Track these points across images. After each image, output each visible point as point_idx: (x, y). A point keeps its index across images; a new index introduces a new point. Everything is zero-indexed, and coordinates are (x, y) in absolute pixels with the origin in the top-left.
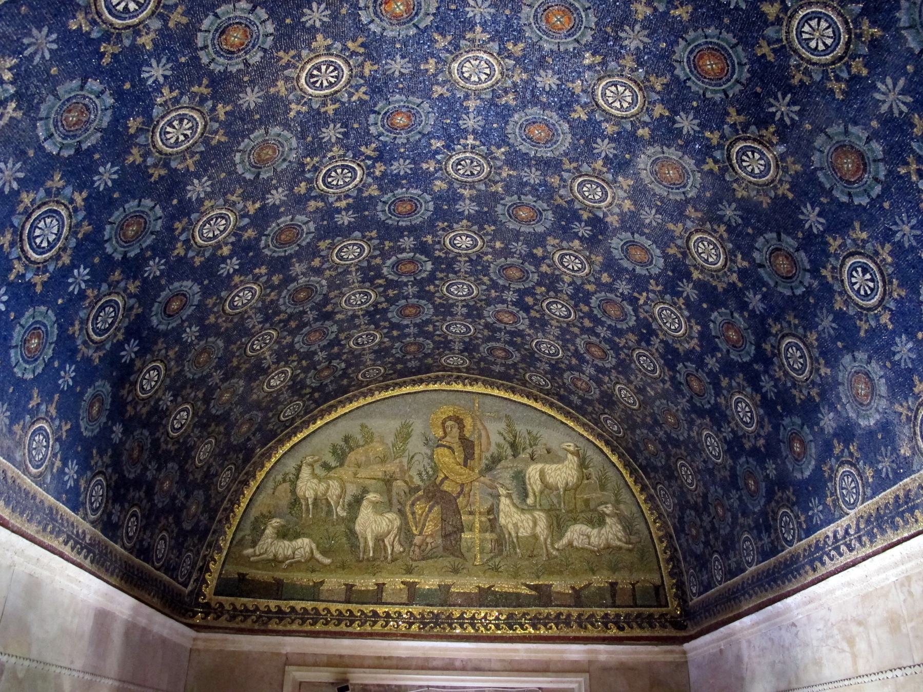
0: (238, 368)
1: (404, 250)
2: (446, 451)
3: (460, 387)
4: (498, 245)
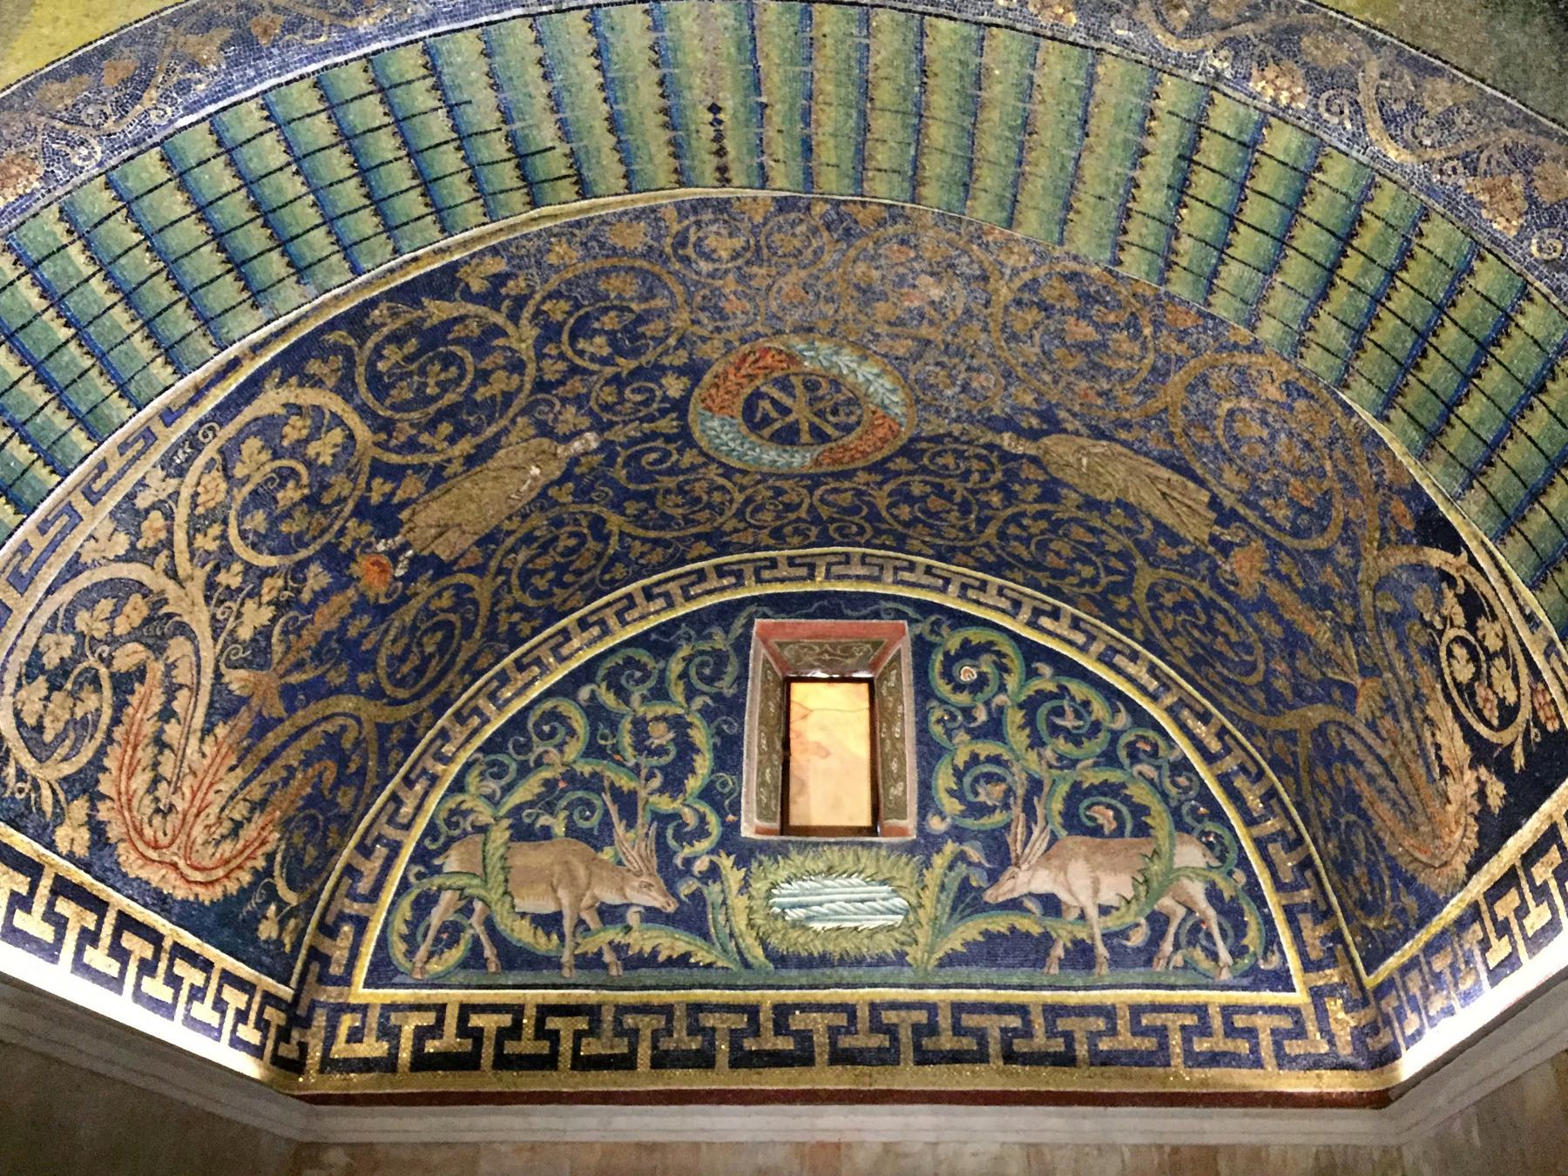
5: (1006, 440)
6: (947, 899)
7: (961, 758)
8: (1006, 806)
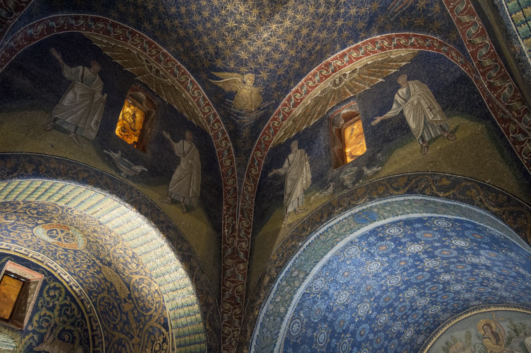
0: (392, 337)
1: (429, 286)
2: (488, 340)
3: (484, 310)
4: (459, 275)
5: (97, 262)
6: (26, 347)
7: (43, 313)
8: (47, 328)
